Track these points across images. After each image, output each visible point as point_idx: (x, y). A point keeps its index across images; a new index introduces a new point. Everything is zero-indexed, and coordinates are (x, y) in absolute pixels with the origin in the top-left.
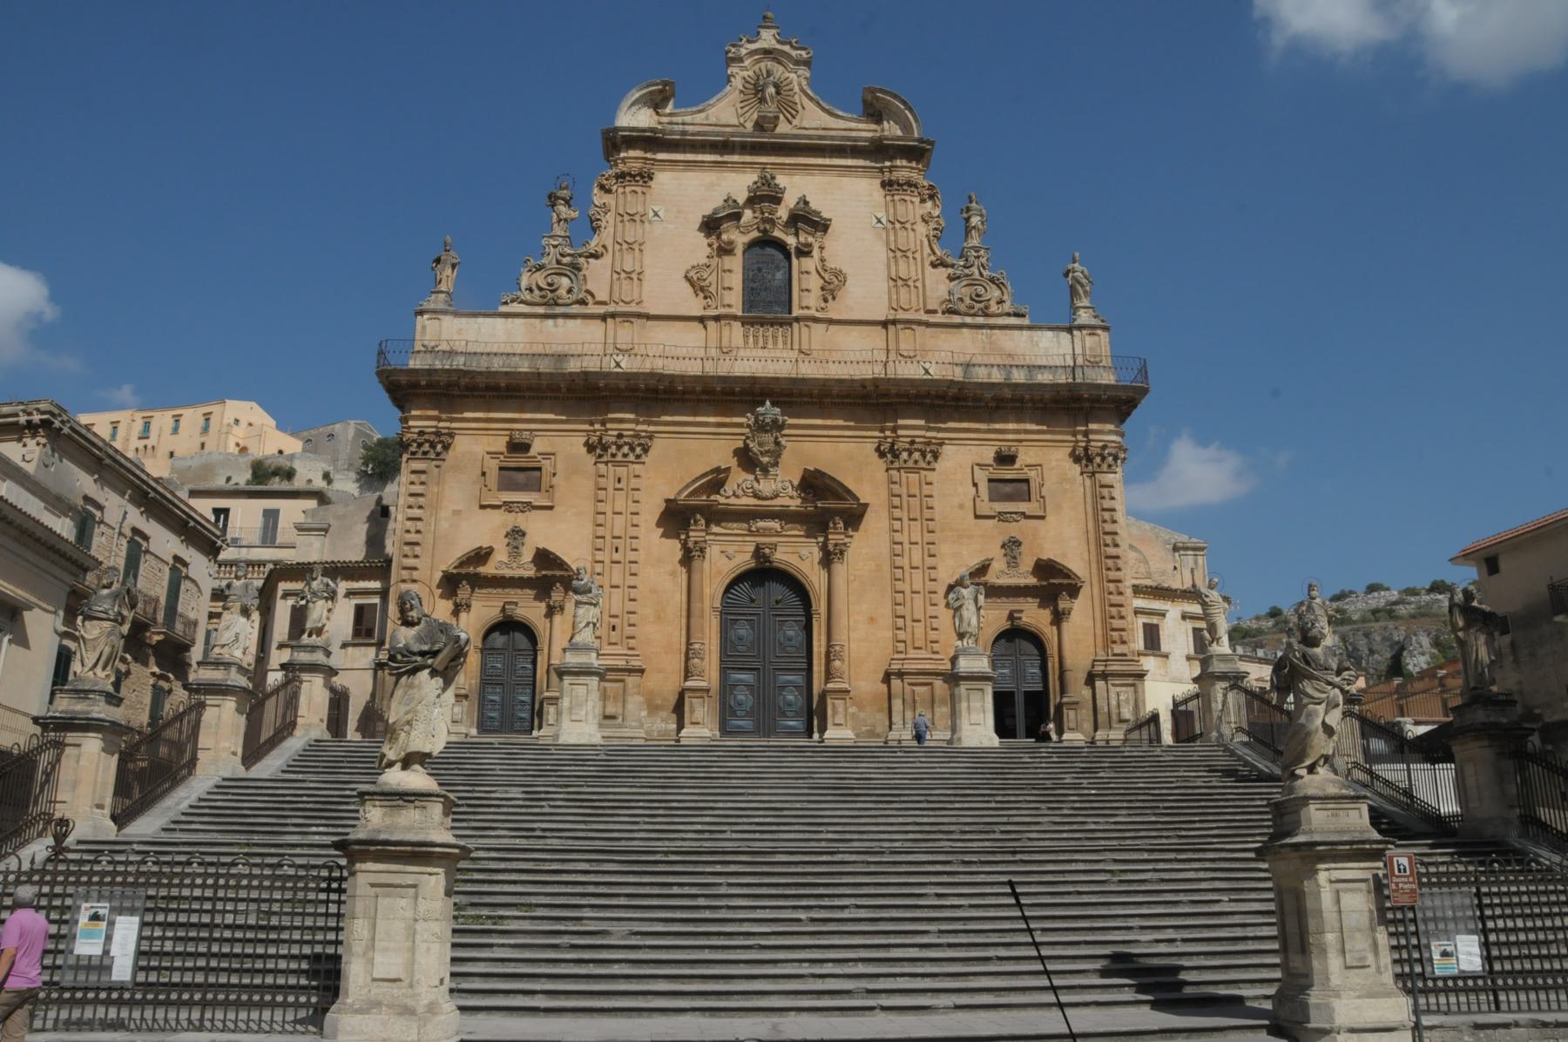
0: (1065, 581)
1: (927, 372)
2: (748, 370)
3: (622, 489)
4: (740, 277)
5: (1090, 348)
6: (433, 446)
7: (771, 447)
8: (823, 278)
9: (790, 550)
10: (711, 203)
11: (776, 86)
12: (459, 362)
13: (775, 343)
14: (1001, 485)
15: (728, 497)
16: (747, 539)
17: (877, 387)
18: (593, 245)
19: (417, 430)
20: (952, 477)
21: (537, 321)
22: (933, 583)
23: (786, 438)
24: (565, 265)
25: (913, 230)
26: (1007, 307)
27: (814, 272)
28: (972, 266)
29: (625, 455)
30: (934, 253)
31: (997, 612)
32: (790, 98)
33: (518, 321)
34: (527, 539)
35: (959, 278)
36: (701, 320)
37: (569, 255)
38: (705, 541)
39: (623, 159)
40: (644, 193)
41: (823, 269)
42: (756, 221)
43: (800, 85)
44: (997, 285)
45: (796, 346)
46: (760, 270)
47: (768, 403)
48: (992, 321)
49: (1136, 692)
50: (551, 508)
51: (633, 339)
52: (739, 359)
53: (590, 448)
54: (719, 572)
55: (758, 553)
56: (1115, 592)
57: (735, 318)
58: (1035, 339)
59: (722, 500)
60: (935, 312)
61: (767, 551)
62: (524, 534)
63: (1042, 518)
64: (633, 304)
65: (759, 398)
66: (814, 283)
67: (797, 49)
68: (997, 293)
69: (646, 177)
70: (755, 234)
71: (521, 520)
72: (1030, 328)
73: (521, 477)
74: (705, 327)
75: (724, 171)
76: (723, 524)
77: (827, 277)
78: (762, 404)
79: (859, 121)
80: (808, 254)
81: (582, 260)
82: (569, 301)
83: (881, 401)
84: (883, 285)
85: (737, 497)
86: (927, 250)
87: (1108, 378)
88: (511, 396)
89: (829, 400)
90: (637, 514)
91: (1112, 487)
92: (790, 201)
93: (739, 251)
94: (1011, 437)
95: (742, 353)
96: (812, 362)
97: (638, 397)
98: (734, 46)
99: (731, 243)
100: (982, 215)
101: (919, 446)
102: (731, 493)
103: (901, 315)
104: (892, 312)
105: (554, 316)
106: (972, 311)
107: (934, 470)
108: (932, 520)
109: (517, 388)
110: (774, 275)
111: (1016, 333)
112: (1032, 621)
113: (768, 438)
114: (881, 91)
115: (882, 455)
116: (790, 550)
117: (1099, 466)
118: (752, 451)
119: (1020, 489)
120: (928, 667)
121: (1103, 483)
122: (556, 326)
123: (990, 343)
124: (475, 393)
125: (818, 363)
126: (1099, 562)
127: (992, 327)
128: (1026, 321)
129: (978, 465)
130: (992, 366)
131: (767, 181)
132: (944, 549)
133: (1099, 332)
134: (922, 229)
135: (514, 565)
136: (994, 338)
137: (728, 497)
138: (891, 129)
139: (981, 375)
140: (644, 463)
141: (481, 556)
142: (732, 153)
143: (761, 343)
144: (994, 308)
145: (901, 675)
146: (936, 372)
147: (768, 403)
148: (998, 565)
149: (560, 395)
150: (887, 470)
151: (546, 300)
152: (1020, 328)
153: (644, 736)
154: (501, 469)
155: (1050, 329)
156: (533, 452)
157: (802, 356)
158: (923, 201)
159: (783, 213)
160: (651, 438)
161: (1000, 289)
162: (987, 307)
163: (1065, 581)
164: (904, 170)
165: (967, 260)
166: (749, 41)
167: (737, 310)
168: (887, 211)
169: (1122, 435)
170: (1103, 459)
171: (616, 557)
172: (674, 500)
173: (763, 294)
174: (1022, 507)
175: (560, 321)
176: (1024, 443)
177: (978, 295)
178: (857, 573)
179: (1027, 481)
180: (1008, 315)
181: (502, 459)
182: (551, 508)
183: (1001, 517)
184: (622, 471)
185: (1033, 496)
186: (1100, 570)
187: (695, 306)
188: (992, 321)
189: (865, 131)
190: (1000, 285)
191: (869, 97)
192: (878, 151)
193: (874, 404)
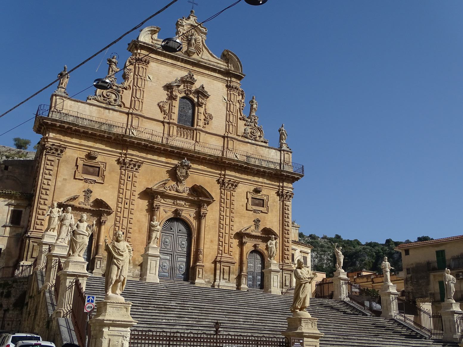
1: (236, 157)
3: (130, 181)
4: (178, 109)
5: (286, 158)
6: (57, 150)
7: (185, 174)
8: (205, 116)
9: (187, 212)
10: (170, 80)
11: (195, 41)
12: (70, 119)
13: (187, 136)
14: (255, 200)
16: (173, 206)
18: (126, 84)
19: (51, 143)
20: (241, 195)
21: (102, 109)
22: (232, 231)
24: (114, 89)
25: (236, 105)
26: (262, 139)
27: (203, 113)
28: (253, 122)
29: (132, 168)
30: (241, 115)
31: (251, 244)
32: (199, 46)
33: (94, 107)
34: (92, 194)
35: (248, 126)
36: (163, 122)
37: (116, 86)
38: (160, 205)
39: (139, 53)
40: (145, 69)
41: (205, 112)
42: (185, 90)
43: (202, 41)
44: (259, 131)
45: (195, 139)
46: (184, 108)
48: (257, 143)
50: (102, 183)
51: (138, 125)
53: (118, 162)
54: (162, 217)
55: (176, 212)
57: (175, 124)
58: (270, 152)
60: (240, 136)
61: (181, 212)
62: (91, 192)
63: (267, 213)
64: (139, 111)
66: (202, 117)
67: (202, 27)
68: (259, 133)
69: (147, 63)
70: (183, 95)
71: (91, 187)
72: (269, 148)
73: (91, 169)
74: (164, 126)
75: (174, 68)
76: (165, 200)
77: (206, 115)
79: (221, 61)
80: (201, 106)
81: (120, 89)
82: (115, 104)
84: (224, 123)
85: (170, 190)
86: (239, 114)
87: (291, 170)
88: (91, 138)
89: (204, 161)
90: (135, 191)
91: (289, 206)
92: (197, 86)
93: (178, 99)
94: (260, 184)
96: (200, 146)
97: (139, 147)
98: (181, 20)
99: (176, 96)
100: (256, 105)
101: (232, 183)
102: (169, 189)
103: (229, 135)
104: (226, 133)
105: (109, 109)
106: (251, 138)
107: (235, 191)
108: (233, 209)
109: (95, 135)
110: (188, 111)
111: (264, 148)
112: (261, 248)
113: (184, 171)
114: (231, 52)
115: (219, 183)
116: (187, 212)
117: (285, 198)
118: (178, 175)
119: (261, 203)
120: (229, 260)
121: (286, 205)
122: (109, 113)
123: (256, 151)
124: (77, 133)
127: (257, 145)
128: (267, 145)
129: (249, 192)
130: (257, 159)
131: (191, 77)
132: (236, 219)
133: (289, 153)
134: (238, 105)
135: (87, 204)
136: (257, 149)
137: (167, 190)
138: (231, 68)
139: (252, 161)
141: (74, 198)
142: (178, 61)
144: (258, 138)
145: (220, 262)
146: (240, 158)
148: (253, 228)
149: (110, 141)
150: (220, 189)
151: (106, 102)
152: (266, 147)
153: (132, 275)
154: (84, 165)
155: (275, 149)
156: (97, 160)
158: (239, 95)
159: (193, 89)
160: (142, 163)
161: (260, 132)
162: (256, 137)
164: (235, 82)
165: (251, 120)
166: (186, 20)
167: (176, 121)
168: (228, 96)
169: (293, 189)
170: (287, 196)
171: (127, 206)
173: (184, 117)
174: (261, 209)
175: (111, 111)
176: (263, 187)
177: (253, 133)
178: (208, 224)
179: (263, 200)
180: (262, 142)
181: (85, 161)
182: (102, 183)
183: (255, 211)
184: (130, 174)
185: (265, 206)
187: (160, 117)
188: (257, 143)
189: (222, 65)
190: (260, 131)
191: (226, 53)
192: (226, 73)
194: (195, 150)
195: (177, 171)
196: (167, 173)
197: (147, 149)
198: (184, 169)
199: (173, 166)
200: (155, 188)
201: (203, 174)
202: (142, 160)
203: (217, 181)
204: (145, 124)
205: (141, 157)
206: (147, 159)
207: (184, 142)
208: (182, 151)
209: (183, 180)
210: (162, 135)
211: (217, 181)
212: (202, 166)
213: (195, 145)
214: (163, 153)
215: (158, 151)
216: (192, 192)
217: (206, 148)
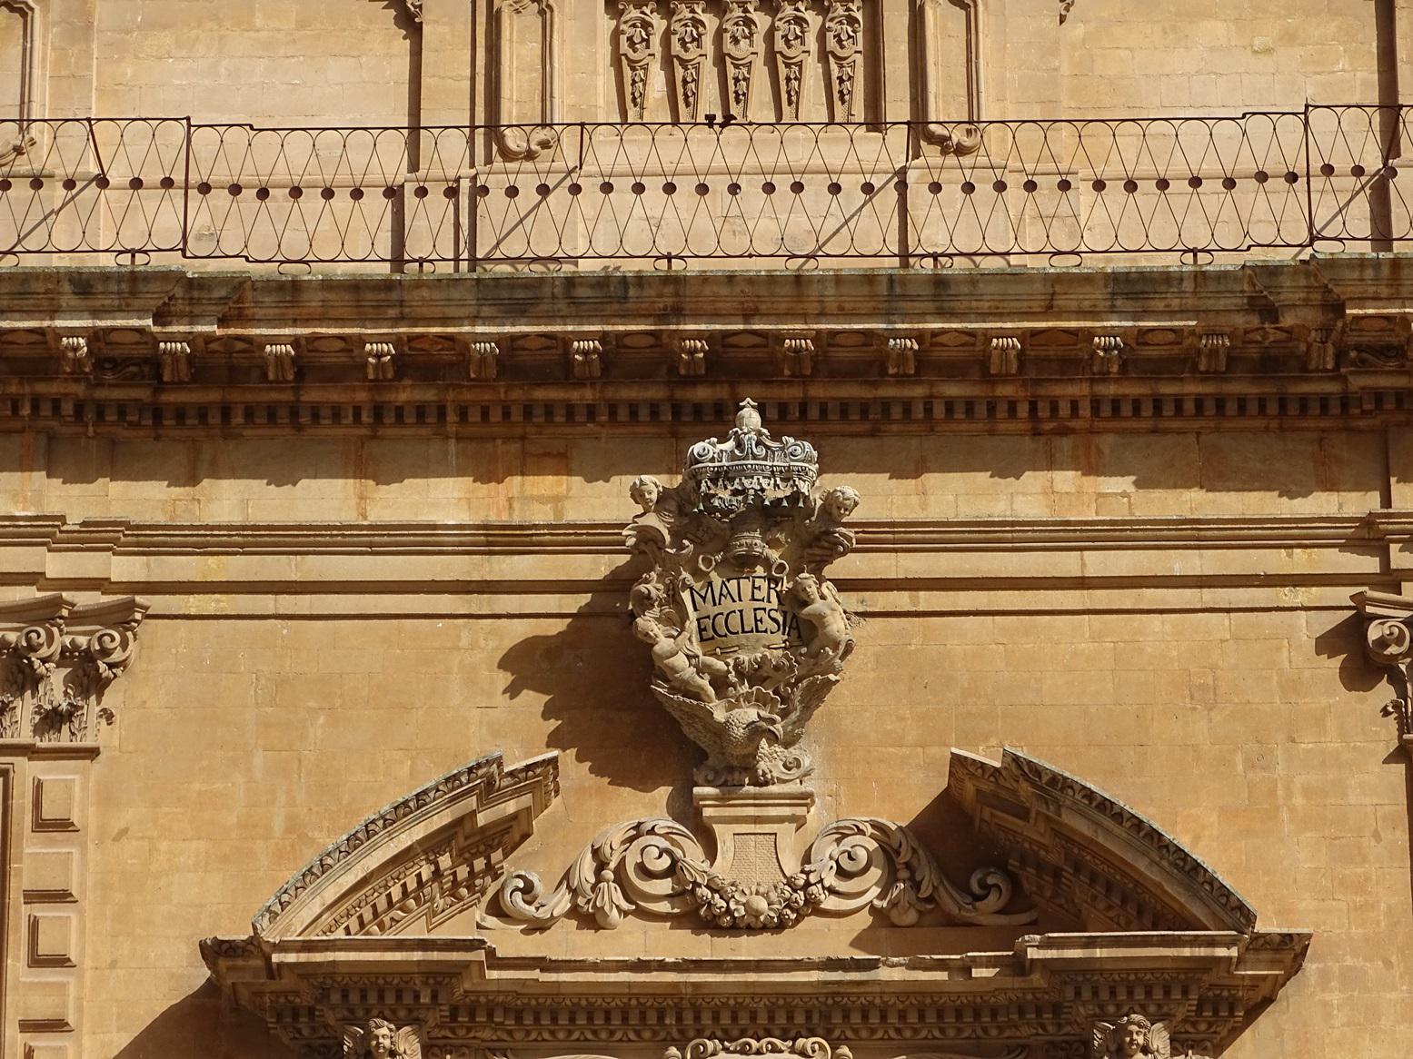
2: (638, 240)
7: (771, 646)
13: (784, 95)
15: (537, 926)
17: (1338, 308)
23: (853, 601)
45: (897, 106)
47: (751, 417)
51: (25, 101)
52: (590, 186)
59: (508, 940)
65: (702, 393)
78: (720, 420)
83: (1358, 382)
85: (590, 920)
95: (605, 153)
96: (984, 189)
102: (562, 902)
118: (666, 675)
125: (1015, 192)
137: (537, 926)
140: (92, 753)
143: (709, 100)
147: (751, 417)
157: (931, 153)
160: (122, 618)
172: (254, 946)
193: (1324, 401)
194: (904, 255)
195: (649, 623)
196: (513, 691)
197: (180, 414)
198: (743, 564)
199: (597, 567)
200: (299, 921)
201: (1082, 583)
202: (124, 568)
203: (1326, 645)
204: (128, 69)
205: (97, 536)
206: (202, 549)
207: (719, 185)
208: (678, 313)
209: (755, 732)
210: (391, 161)
211: (1326, 645)
212: (1066, 480)
213: (902, 186)
214: (421, 411)
215: (334, 396)
216: (928, 877)
217: (1083, 192)
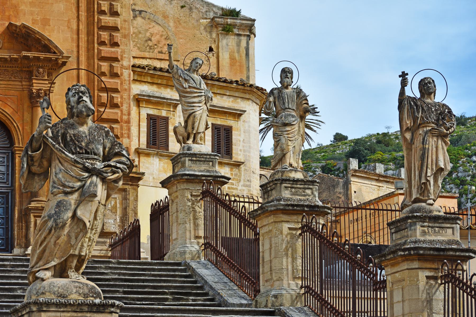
0: (42, 55)
49: (125, 198)
56: (107, 73)
126: (90, 33)
163: (42, 55)
186: (90, 42)
